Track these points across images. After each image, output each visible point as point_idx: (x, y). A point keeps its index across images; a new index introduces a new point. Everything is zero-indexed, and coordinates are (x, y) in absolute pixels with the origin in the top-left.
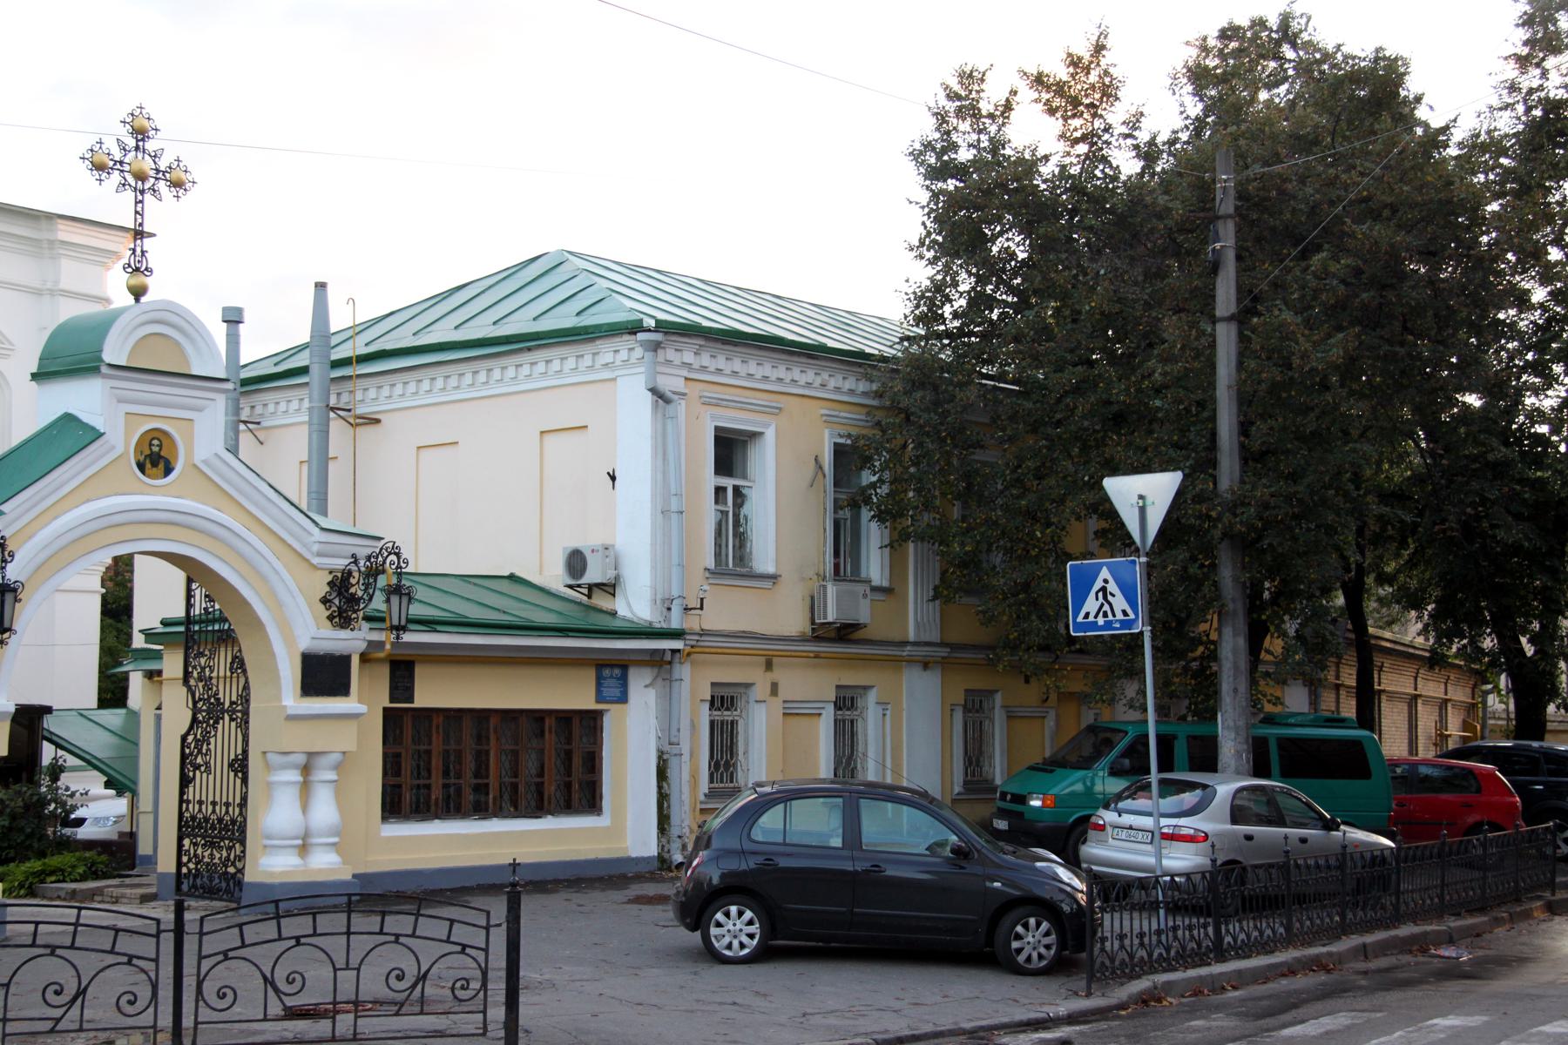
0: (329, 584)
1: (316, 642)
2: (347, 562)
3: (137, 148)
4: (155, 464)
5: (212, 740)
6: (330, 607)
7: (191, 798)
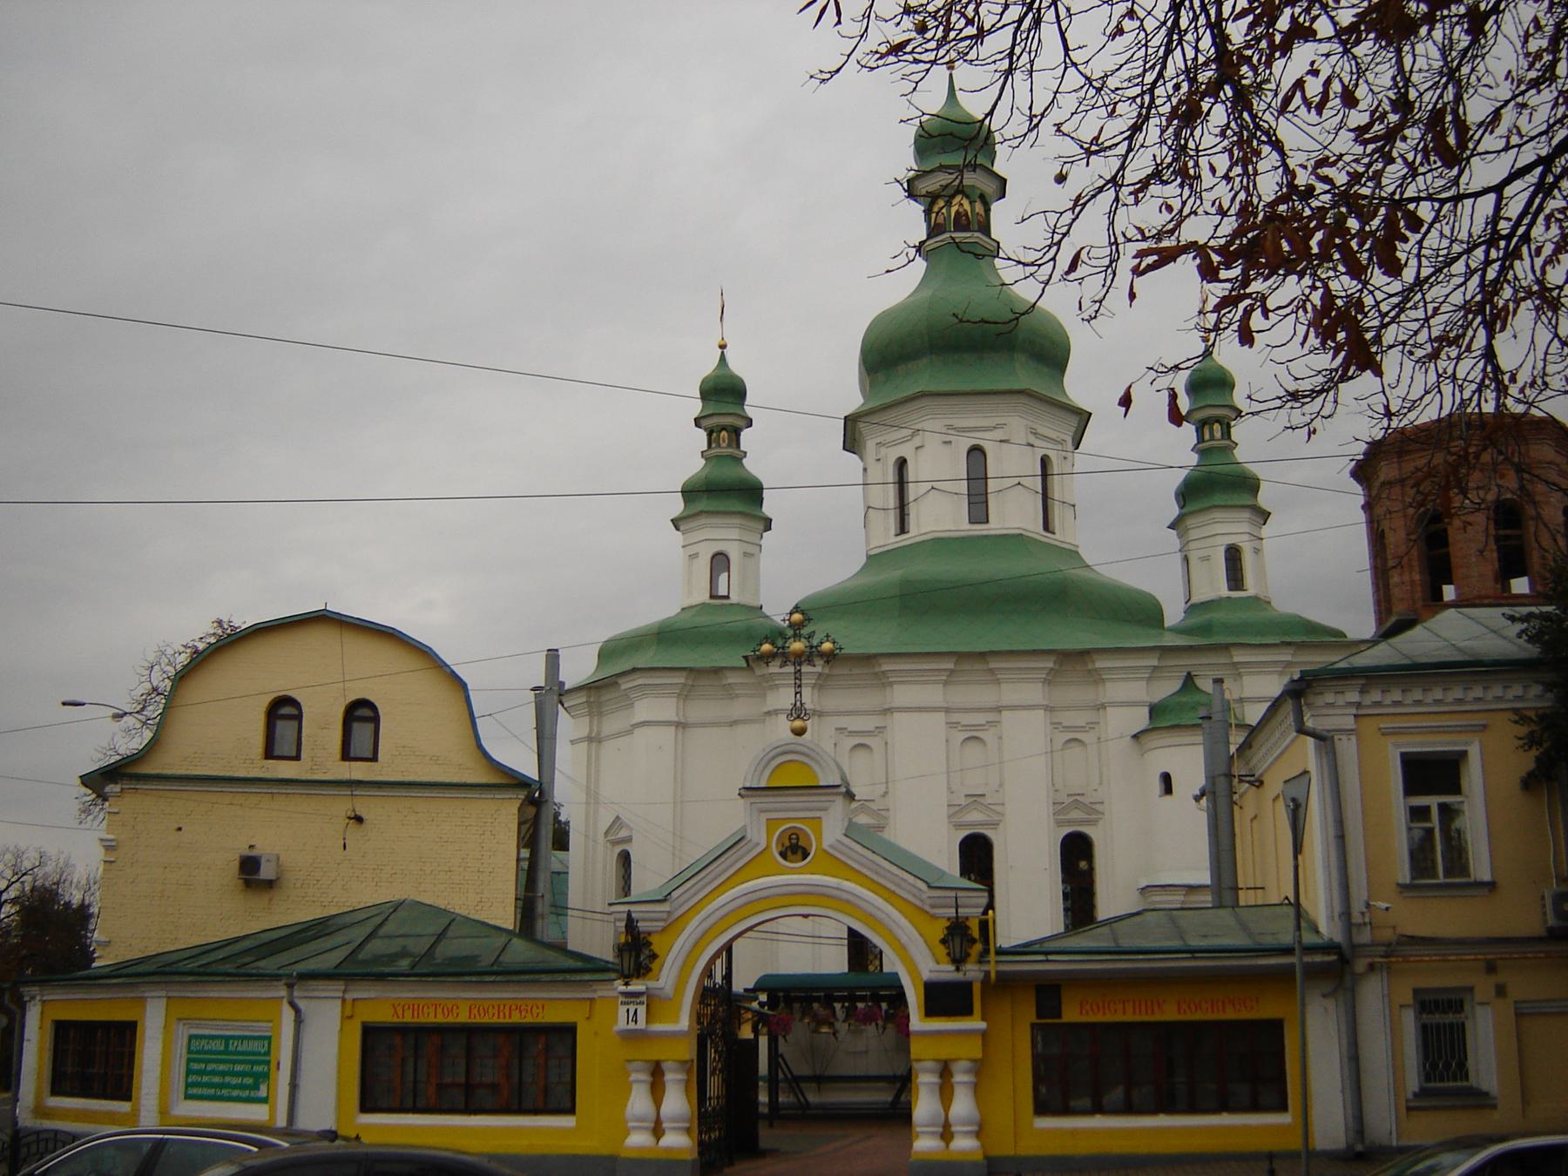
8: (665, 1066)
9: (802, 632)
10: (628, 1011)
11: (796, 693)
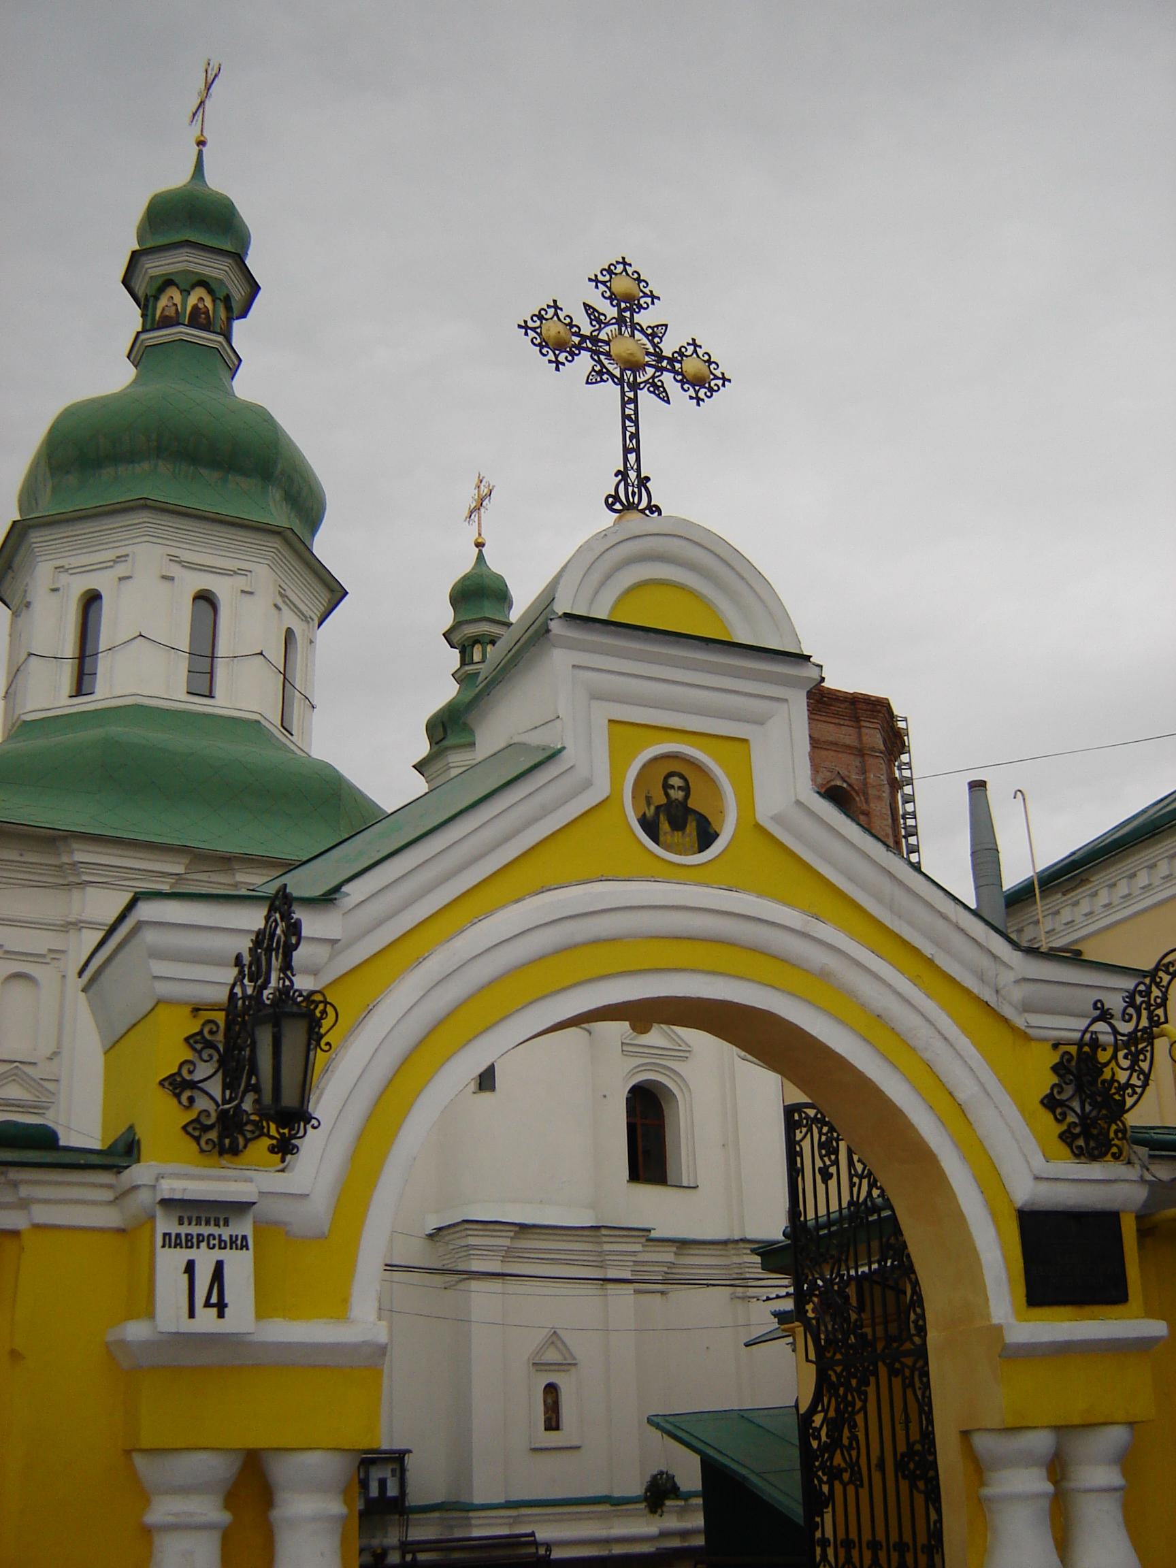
0: (1055, 1069)
1: (1043, 1187)
2: (1082, 1024)
3: (620, 321)
4: (678, 825)
5: (859, 1419)
6: (1064, 1115)
7: (829, 1534)
8: (283, 1470)
9: (637, 318)
10: (190, 1268)
11: (627, 451)
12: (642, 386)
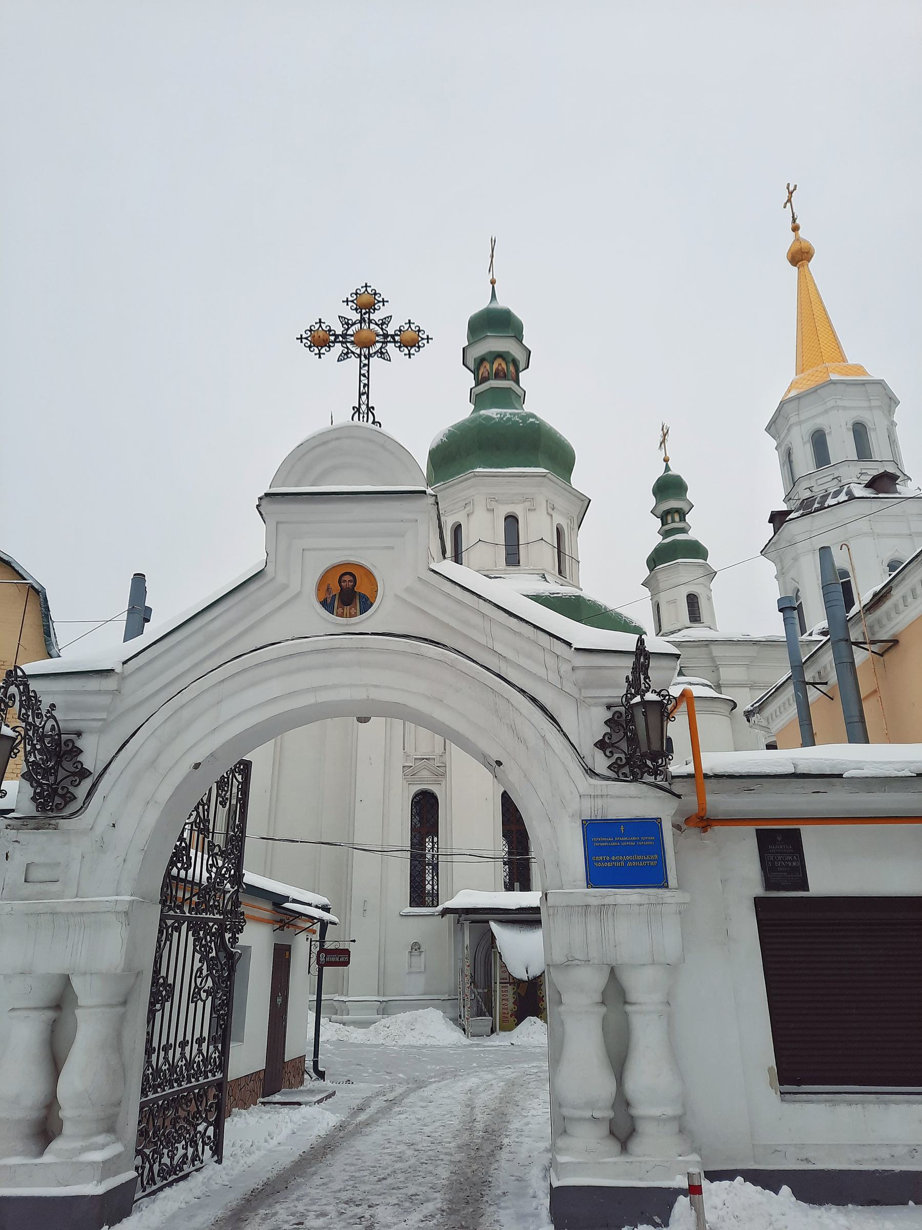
0: (607, 723)
3: (362, 320)
11: (360, 395)
12: (373, 355)
